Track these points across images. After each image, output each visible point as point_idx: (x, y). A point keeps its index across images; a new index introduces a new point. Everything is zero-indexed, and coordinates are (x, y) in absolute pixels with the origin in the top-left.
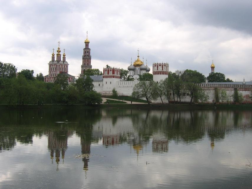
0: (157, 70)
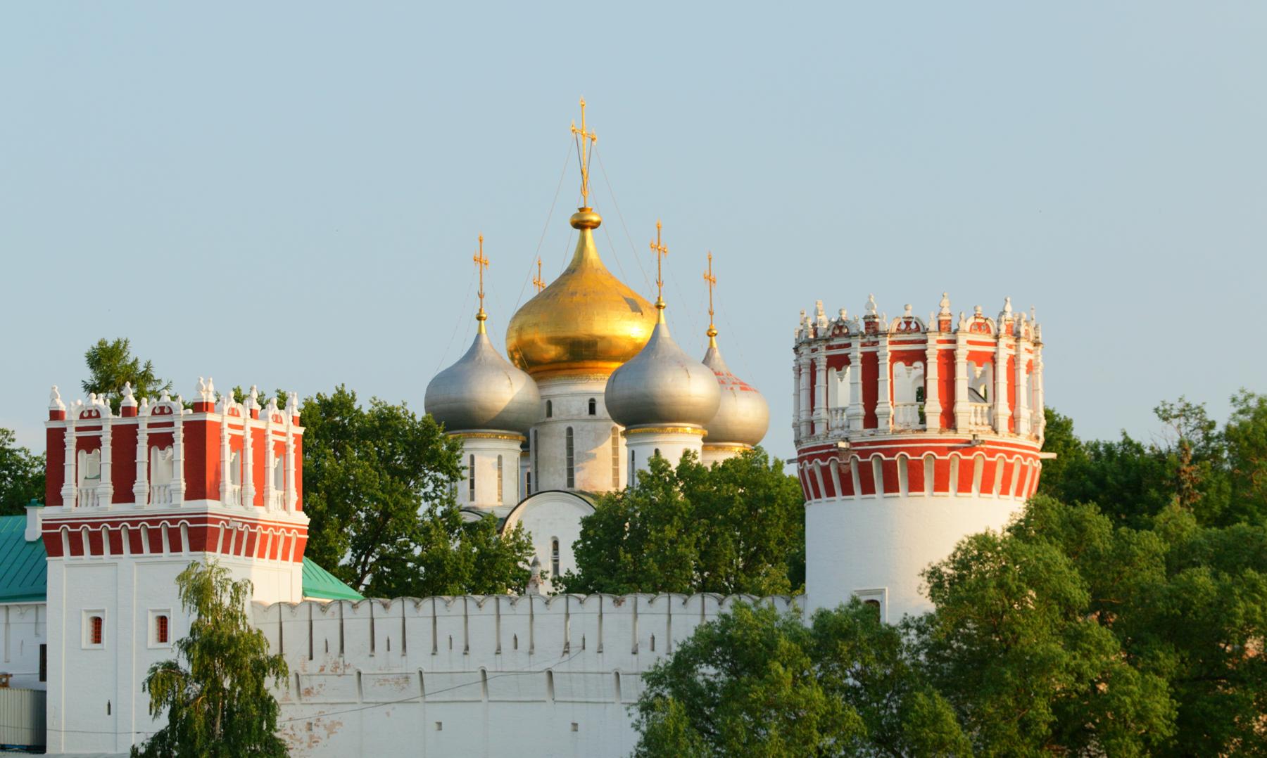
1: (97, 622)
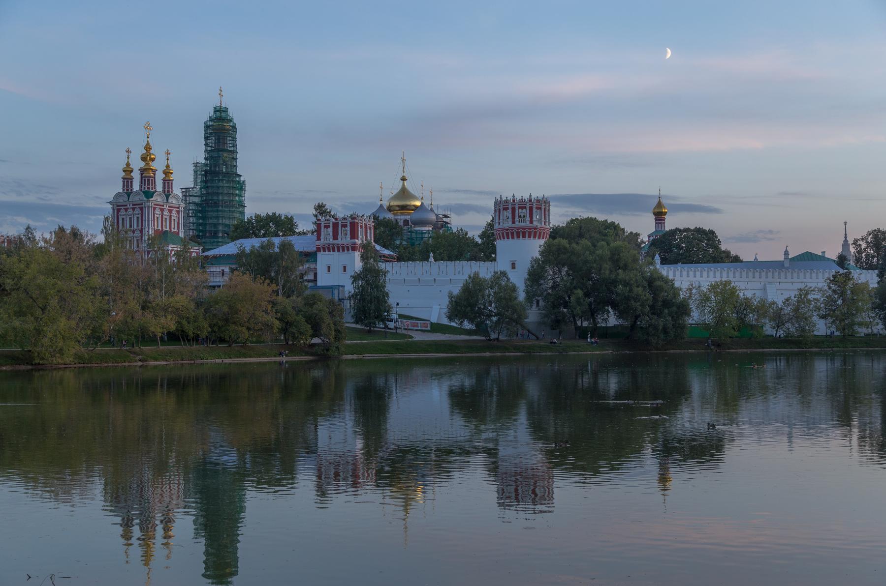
0: (514, 222)
1: (329, 268)
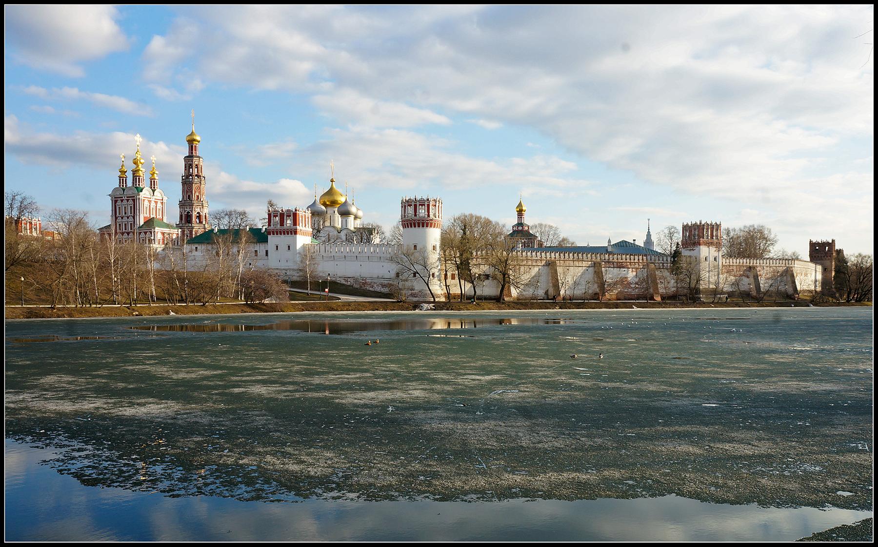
0: (415, 215)
